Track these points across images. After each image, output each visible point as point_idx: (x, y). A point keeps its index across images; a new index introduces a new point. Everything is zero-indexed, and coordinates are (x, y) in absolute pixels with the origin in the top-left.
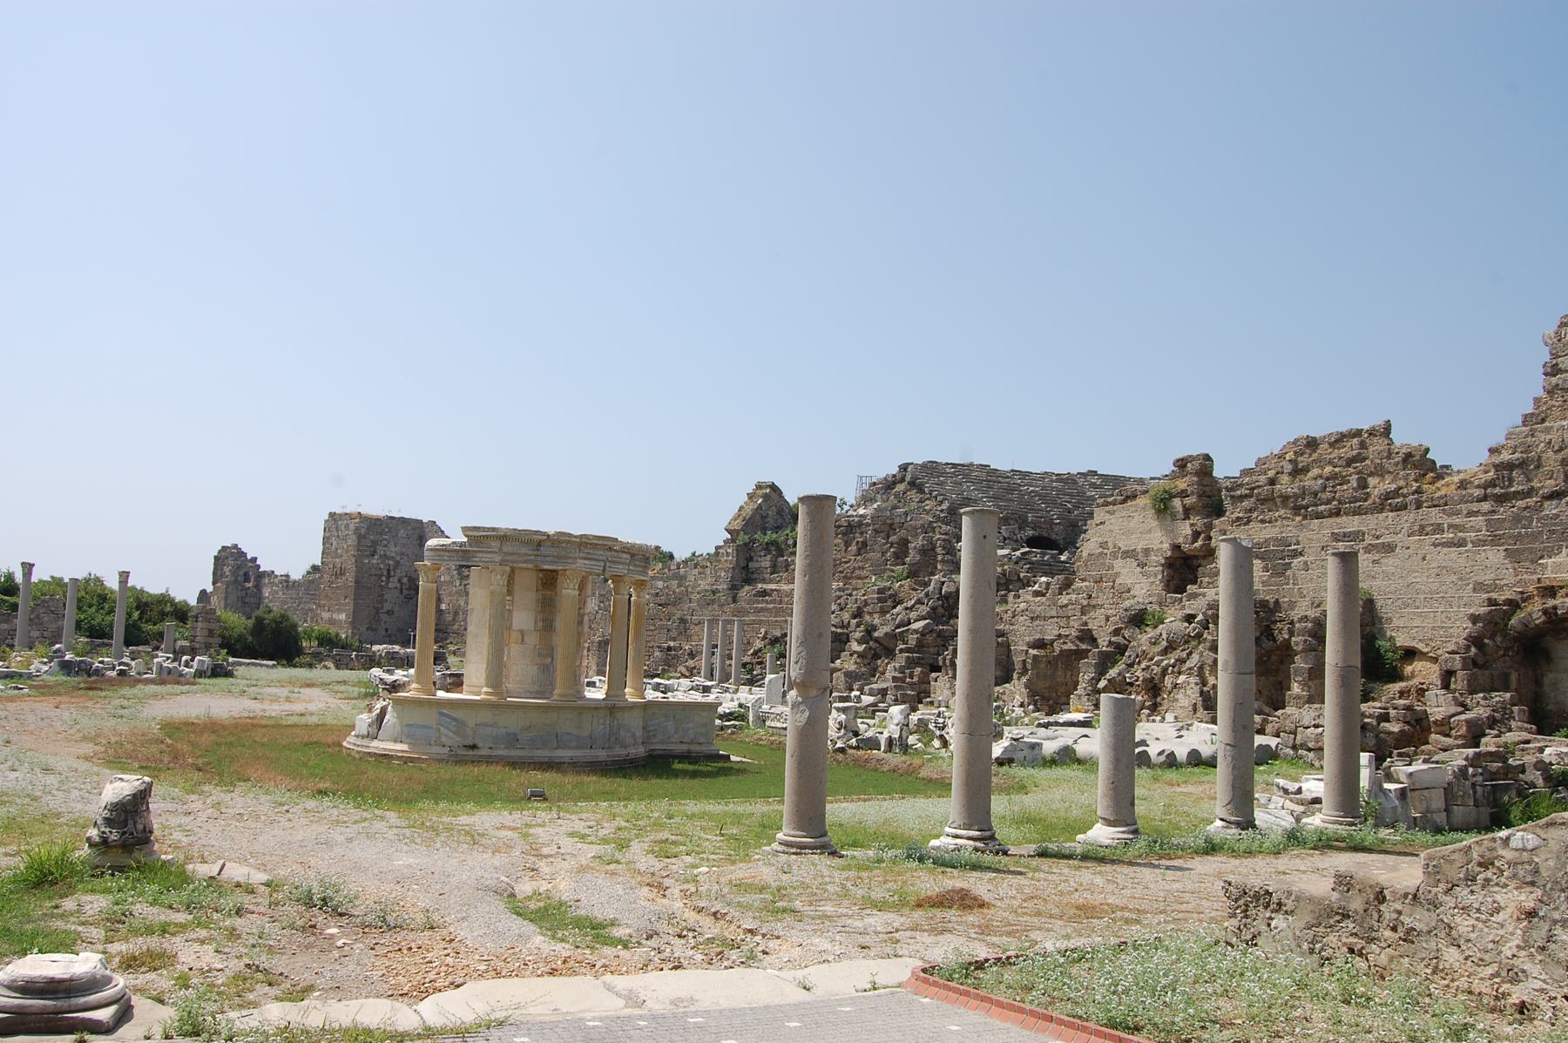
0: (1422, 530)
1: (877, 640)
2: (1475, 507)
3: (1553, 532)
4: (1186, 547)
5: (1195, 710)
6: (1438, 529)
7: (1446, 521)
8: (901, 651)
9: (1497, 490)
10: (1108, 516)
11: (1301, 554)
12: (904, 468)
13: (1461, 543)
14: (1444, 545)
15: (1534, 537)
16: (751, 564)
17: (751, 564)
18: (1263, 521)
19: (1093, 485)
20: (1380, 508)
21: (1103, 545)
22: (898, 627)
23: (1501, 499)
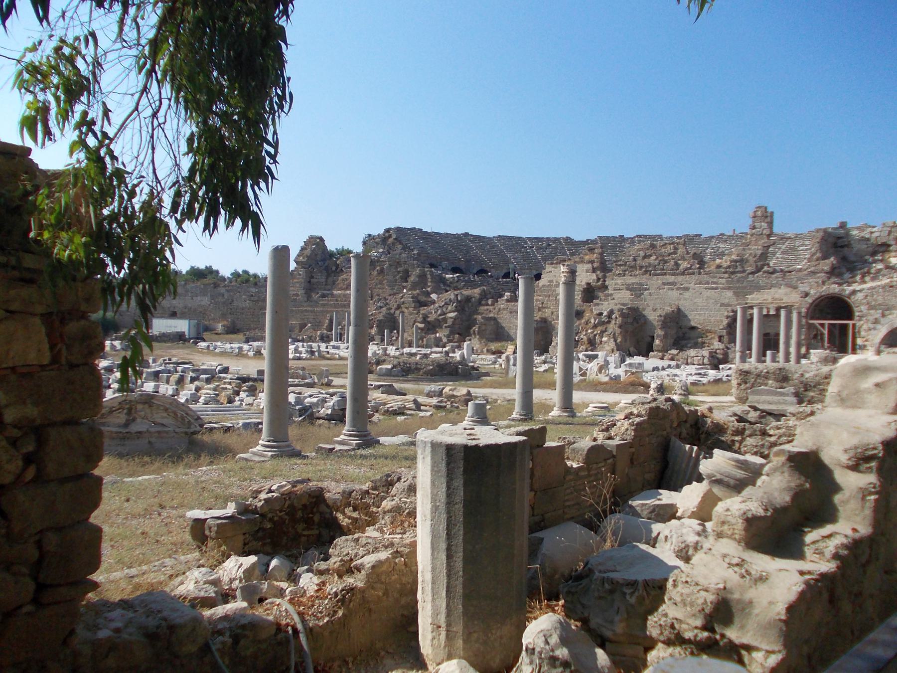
0: (700, 283)
1: (429, 322)
2: (722, 275)
3: (751, 286)
4: (593, 284)
5: (613, 351)
6: (707, 283)
7: (711, 280)
8: (446, 327)
9: (731, 270)
10: (553, 269)
11: (648, 289)
12: (388, 230)
13: (716, 288)
14: (709, 289)
15: (745, 288)
16: (312, 280)
17: (312, 280)
18: (631, 275)
19: (470, 240)
20: (683, 274)
21: (551, 281)
22: (440, 315)
23: (733, 273)
